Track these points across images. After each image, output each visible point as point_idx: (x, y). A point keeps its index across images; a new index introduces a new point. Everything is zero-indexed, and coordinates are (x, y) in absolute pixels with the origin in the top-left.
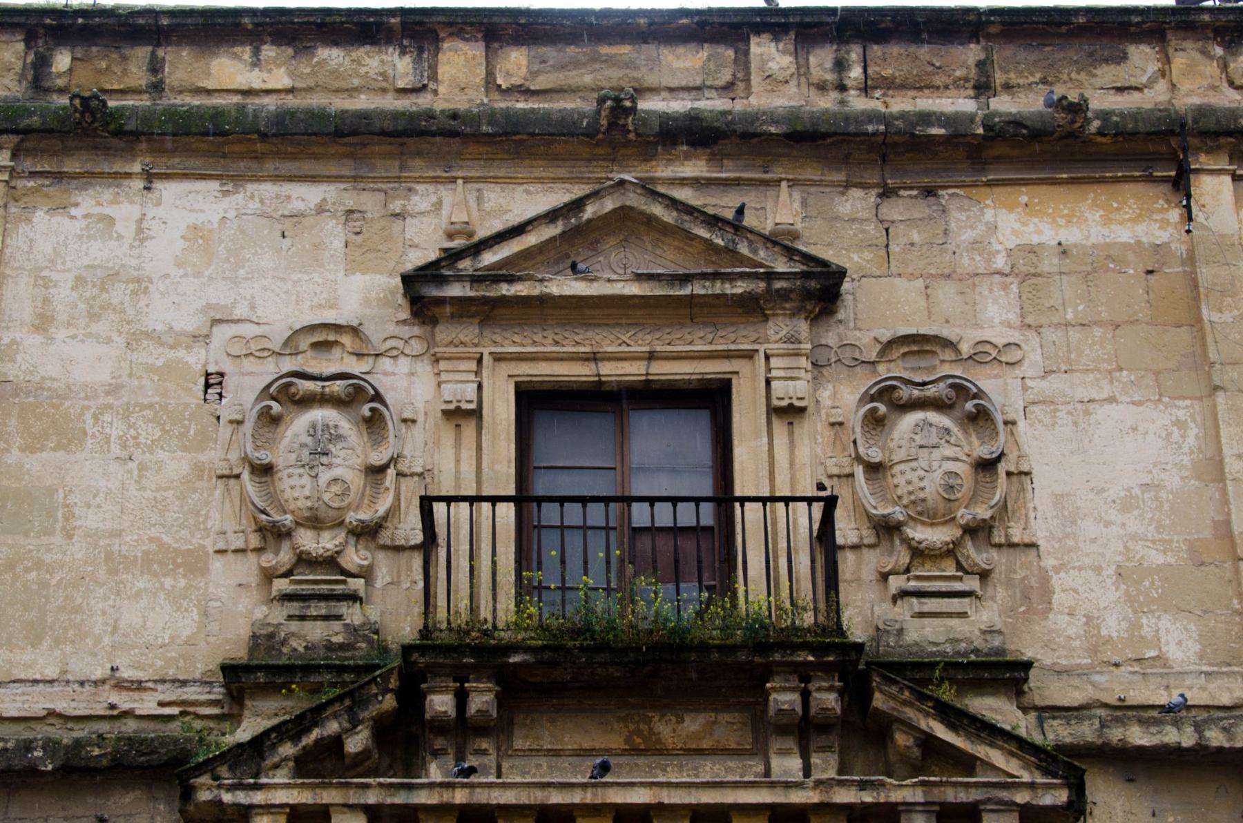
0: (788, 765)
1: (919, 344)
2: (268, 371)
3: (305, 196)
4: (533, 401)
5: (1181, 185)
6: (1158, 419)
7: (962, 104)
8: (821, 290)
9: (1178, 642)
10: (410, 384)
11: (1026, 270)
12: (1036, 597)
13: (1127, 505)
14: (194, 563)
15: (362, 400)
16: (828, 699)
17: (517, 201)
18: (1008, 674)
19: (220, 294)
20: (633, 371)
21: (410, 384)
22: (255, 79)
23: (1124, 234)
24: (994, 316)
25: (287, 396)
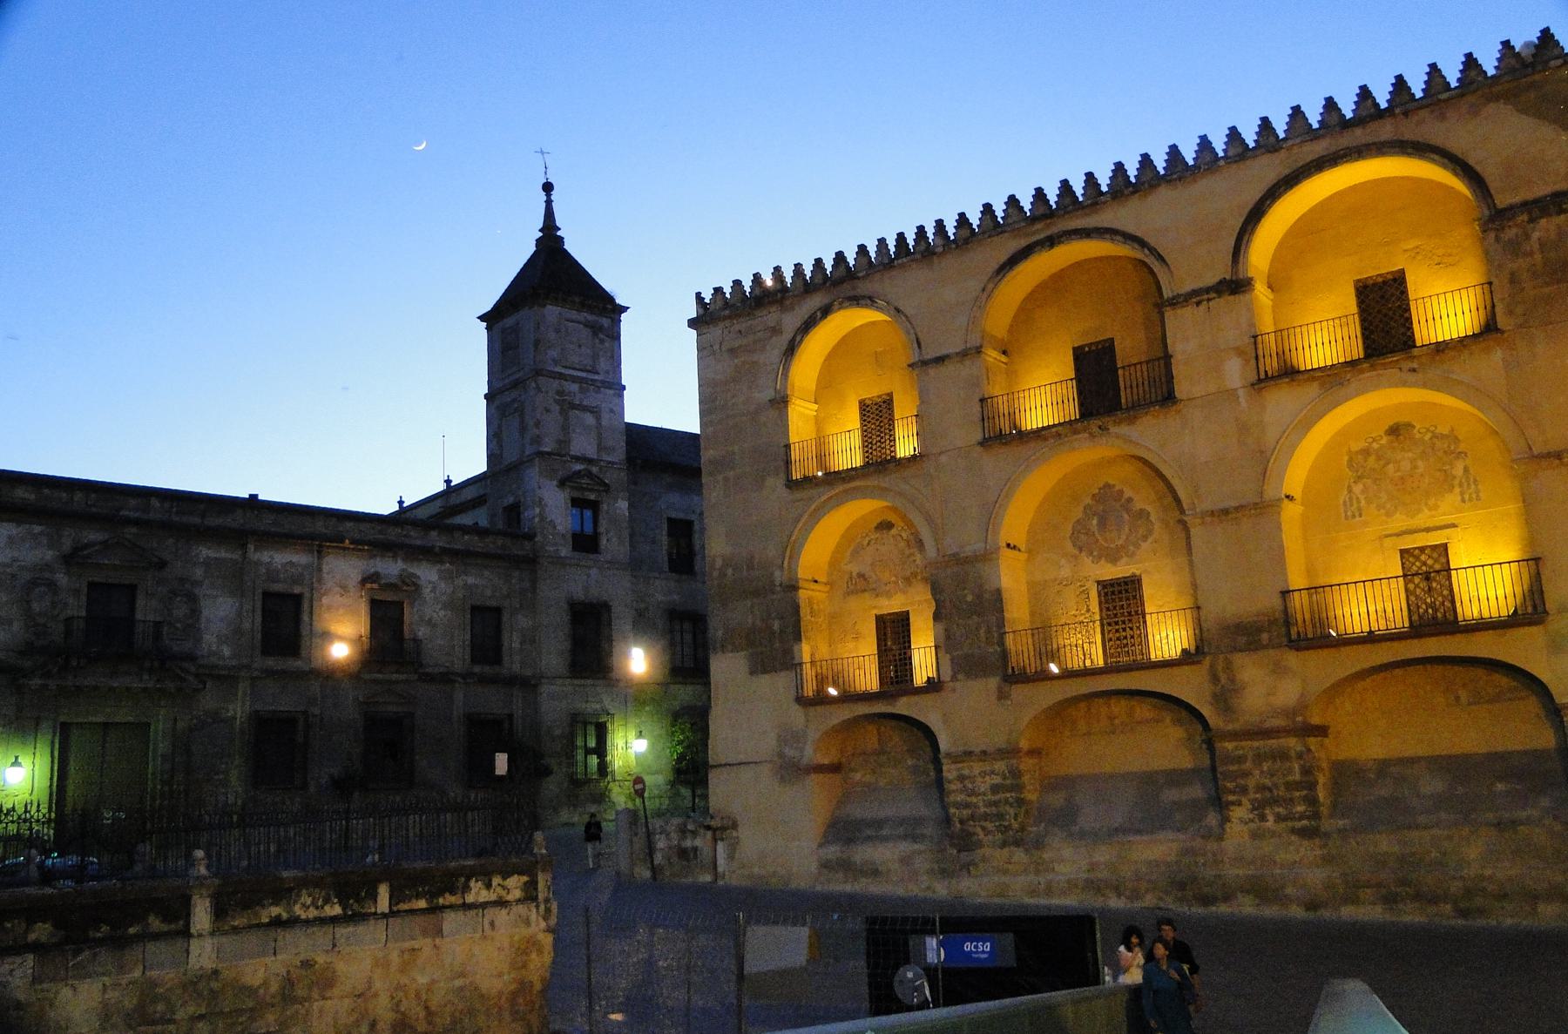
0: (146, 677)
1: (182, 580)
2: (27, 576)
3: (37, 529)
4: (91, 585)
5: (244, 546)
6: (230, 601)
7: (197, 520)
8: (162, 565)
9: (227, 651)
10: (62, 579)
11: (207, 564)
12: (199, 640)
13: (221, 620)
14: (10, 622)
15: (52, 585)
16: (156, 664)
17: (93, 536)
18: (192, 658)
19: (16, 554)
20: (116, 581)
21: (62, 579)
22: (26, 495)
23: (229, 555)
24: (199, 573)
25: (34, 583)
